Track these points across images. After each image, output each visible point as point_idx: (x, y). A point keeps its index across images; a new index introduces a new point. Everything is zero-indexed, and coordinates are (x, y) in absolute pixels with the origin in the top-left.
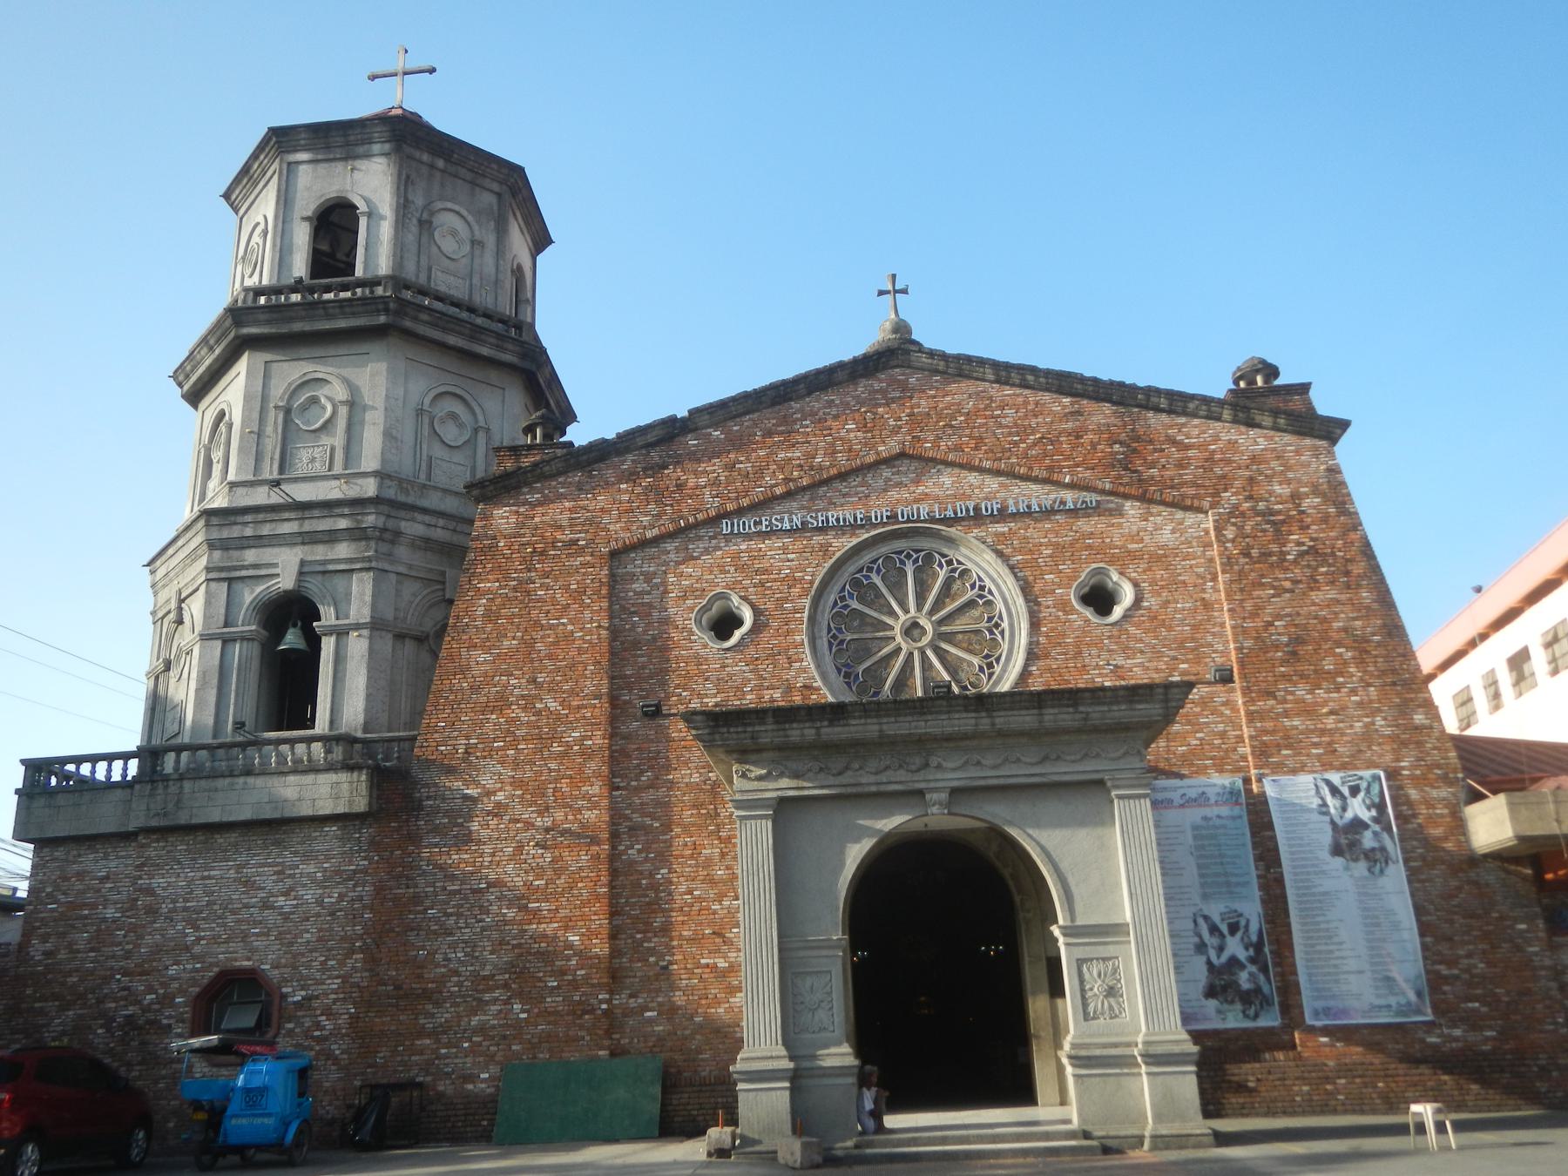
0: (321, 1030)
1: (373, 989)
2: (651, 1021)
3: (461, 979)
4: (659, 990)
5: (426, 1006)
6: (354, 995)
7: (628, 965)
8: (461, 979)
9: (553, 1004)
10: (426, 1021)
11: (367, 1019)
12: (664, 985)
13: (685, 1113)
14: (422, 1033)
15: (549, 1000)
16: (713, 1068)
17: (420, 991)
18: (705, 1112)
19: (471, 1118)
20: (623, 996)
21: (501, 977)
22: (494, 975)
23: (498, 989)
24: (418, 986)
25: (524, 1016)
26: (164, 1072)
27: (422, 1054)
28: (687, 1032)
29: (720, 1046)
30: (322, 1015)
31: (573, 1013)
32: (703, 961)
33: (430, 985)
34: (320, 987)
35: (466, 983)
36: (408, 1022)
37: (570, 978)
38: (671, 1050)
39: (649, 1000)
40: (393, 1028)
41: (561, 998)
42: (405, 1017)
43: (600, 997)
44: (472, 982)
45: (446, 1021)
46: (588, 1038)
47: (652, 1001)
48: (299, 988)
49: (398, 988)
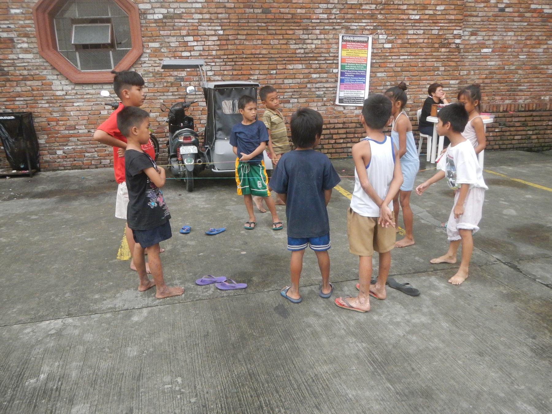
0: (190, 51)
1: (240, 11)
2: (486, 57)
3: (330, 6)
4: (494, 30)
5: (297, 32)
6: (220, 16)
7: (473, 5)
8: (330, 6)
9: (415, 37)
10: (297, 46)
11: (237, 42)
12: (500, 26)
13: (524, 133)
14: (293, 58)
15: (411, 32)
16: (528, 97)
17: (289, 16)
18: (537, 131)
19: (352, 136)
20: (466, 33)
21: (367, 7)
22: (361, 5)
23: (365, 19)
24: (287, 11)
25: (389, 46)
26: (18, 89)
27: (295, 78)
28: (513, 67)
29: (535, 80)
30: (188, 35)
31: (431, 46)
32: (533, 6)
33: (299, 11)
34: (182, 5)
35: (334, 11)
36: (279, 46)
37: (431, 12)
38: (499, 82)
39: (486, 38)
40: (264, 52)
41: (422, 32)
42: (276, 42)
43: (455, 32)
44: (341, 9)
45: (316, 48)
46: (442, 69)
47: (489, 40)
48: (158, 5)
49: (266, 11)
